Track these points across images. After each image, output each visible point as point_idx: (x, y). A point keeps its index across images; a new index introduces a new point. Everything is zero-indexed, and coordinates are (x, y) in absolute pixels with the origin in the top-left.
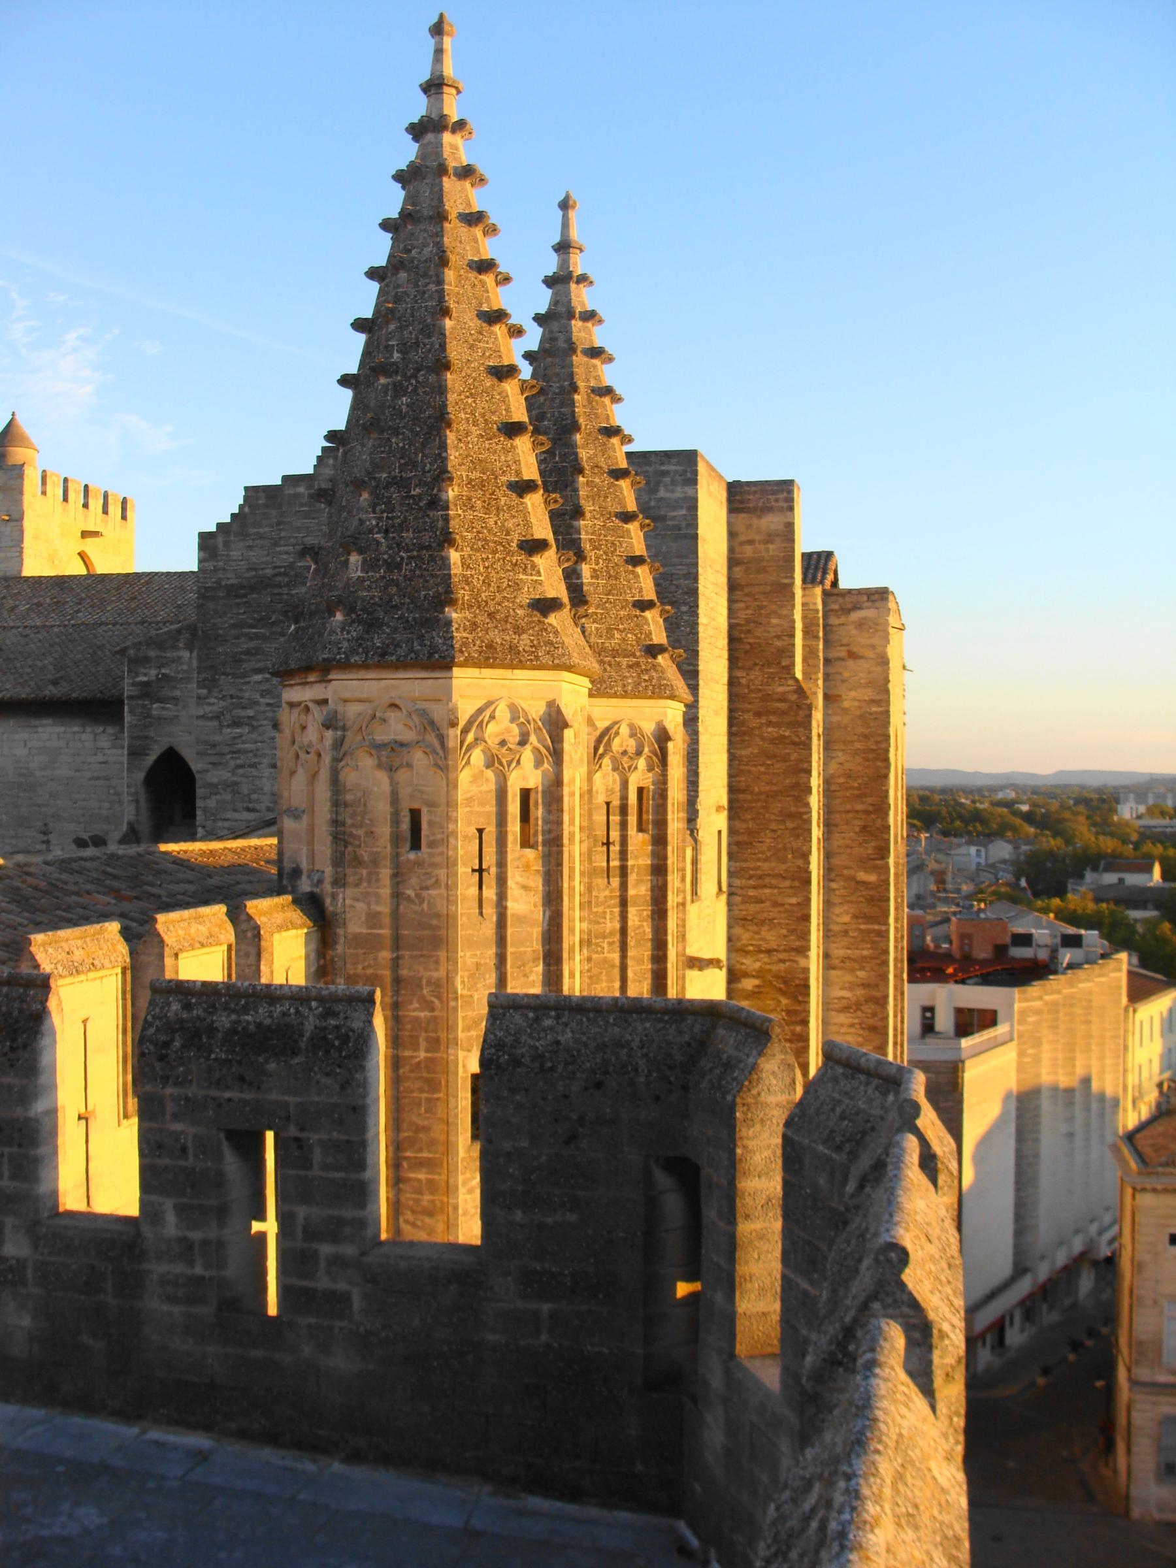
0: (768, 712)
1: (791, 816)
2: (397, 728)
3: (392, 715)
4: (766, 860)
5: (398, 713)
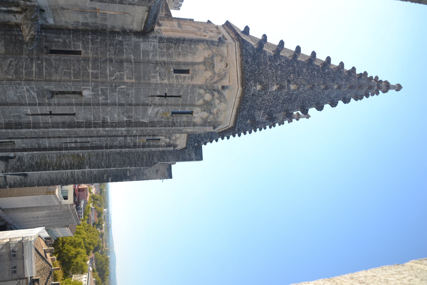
1: (124, 163)
2: (219, 66)
3: (223, 65)
4: (113, 157)
5: (224, 67)
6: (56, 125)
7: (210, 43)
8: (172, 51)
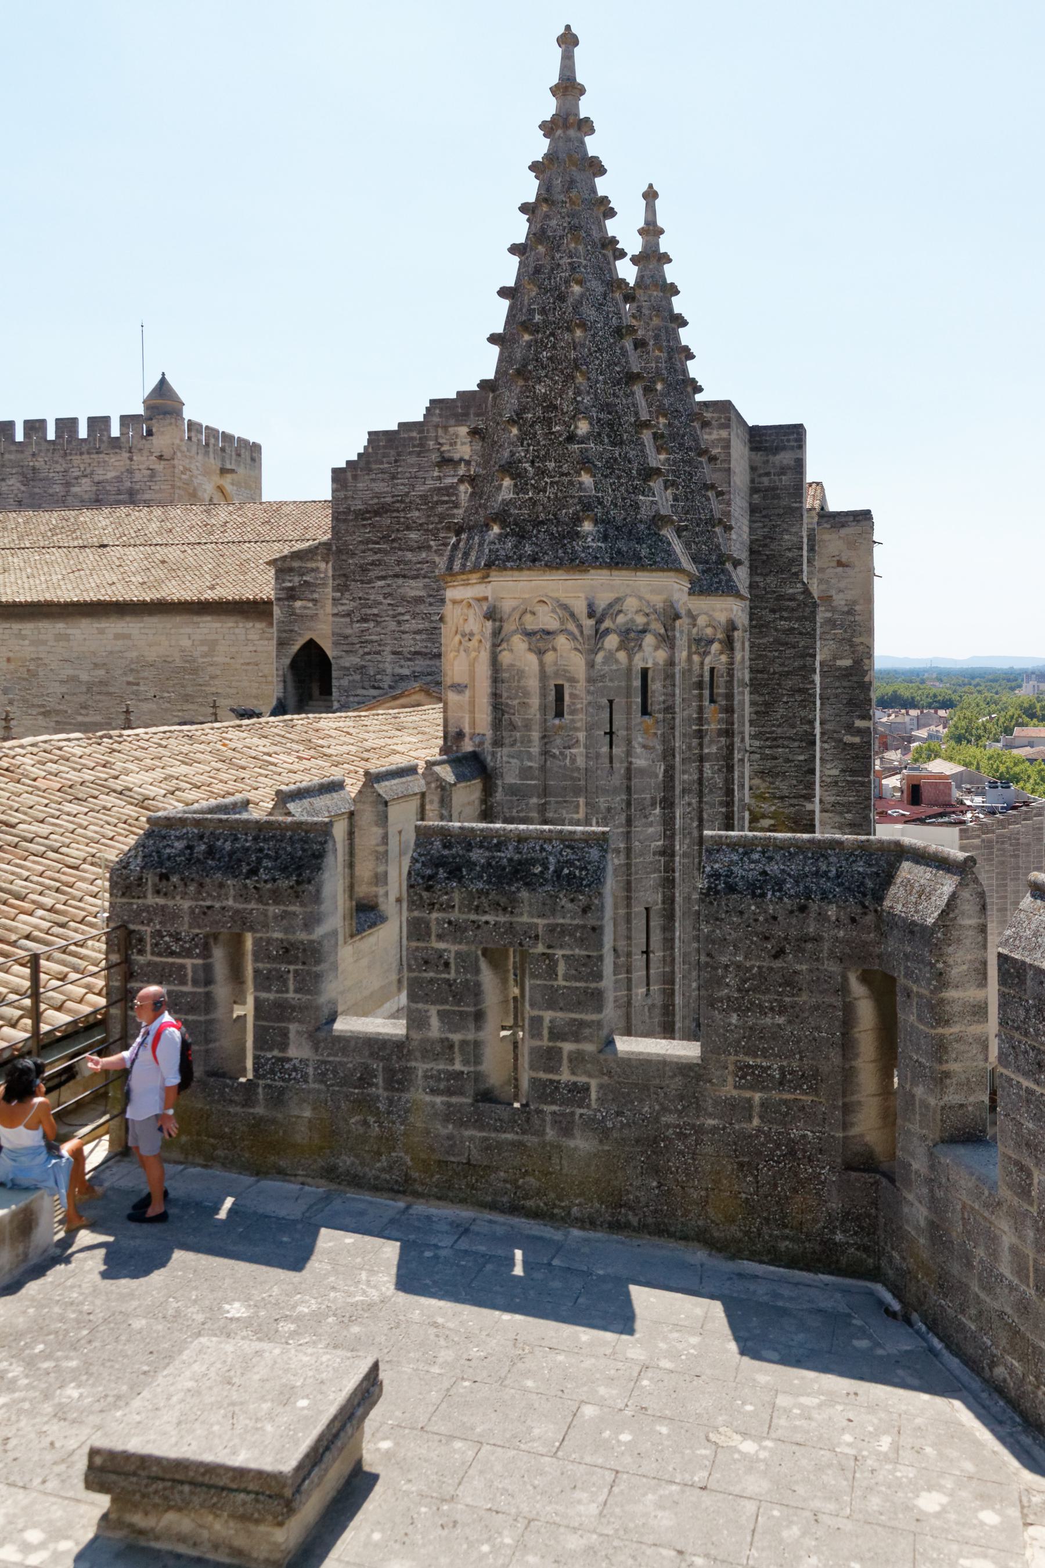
0: (781, 609)
3: (541, 609)
4: (779, 726)
5: (545, 608)
6: (669, 943)
7: (498, 639)
8: (517, 720)
